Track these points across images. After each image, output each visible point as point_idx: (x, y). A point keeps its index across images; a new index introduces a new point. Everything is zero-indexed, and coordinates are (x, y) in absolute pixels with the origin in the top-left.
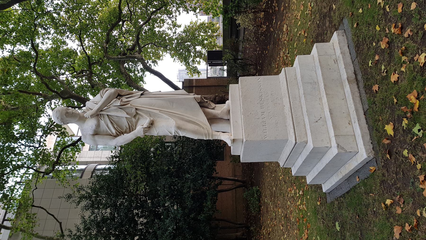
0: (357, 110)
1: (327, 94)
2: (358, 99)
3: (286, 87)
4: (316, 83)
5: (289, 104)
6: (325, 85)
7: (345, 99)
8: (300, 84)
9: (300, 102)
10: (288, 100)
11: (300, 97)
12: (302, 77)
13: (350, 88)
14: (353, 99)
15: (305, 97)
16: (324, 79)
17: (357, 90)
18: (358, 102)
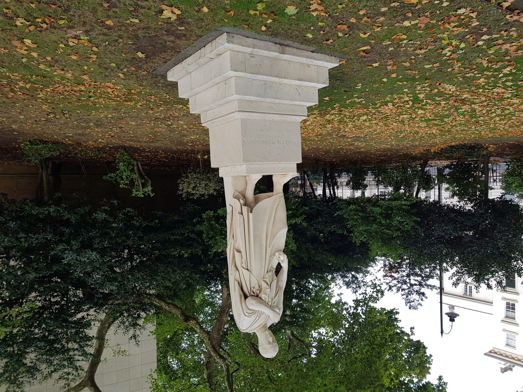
0: (308, 57)
1: (285, 78)
2: (298, 51)
3: (259, 114)
4: (265, 83)
5: (276, 115)
6: (277, 77)
7: (289, 62)
8: (263, 99)
9: (274, 104)
10: (272, 115)
11: (269, 103)
12: (259, 96)
13: (289, 54)
14: (299, 56)
15: (278, 99)
16: (271, 75)
17: (291, 49)
18: (301, 53)
